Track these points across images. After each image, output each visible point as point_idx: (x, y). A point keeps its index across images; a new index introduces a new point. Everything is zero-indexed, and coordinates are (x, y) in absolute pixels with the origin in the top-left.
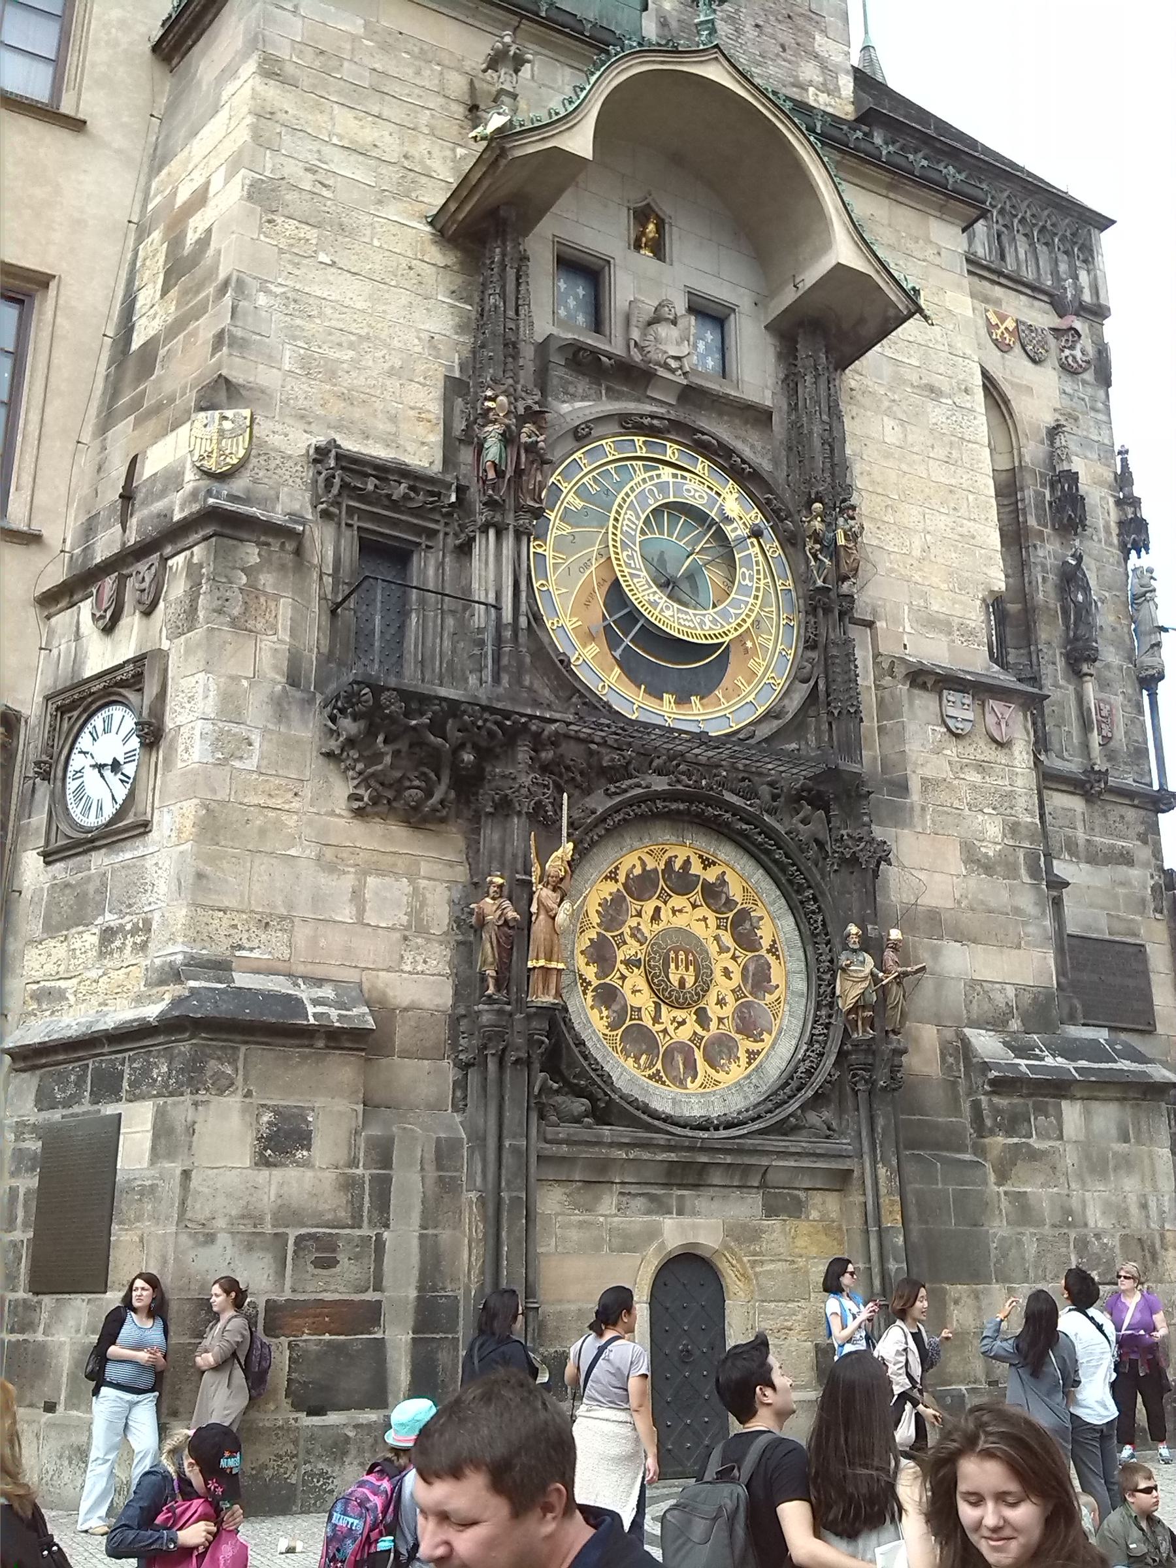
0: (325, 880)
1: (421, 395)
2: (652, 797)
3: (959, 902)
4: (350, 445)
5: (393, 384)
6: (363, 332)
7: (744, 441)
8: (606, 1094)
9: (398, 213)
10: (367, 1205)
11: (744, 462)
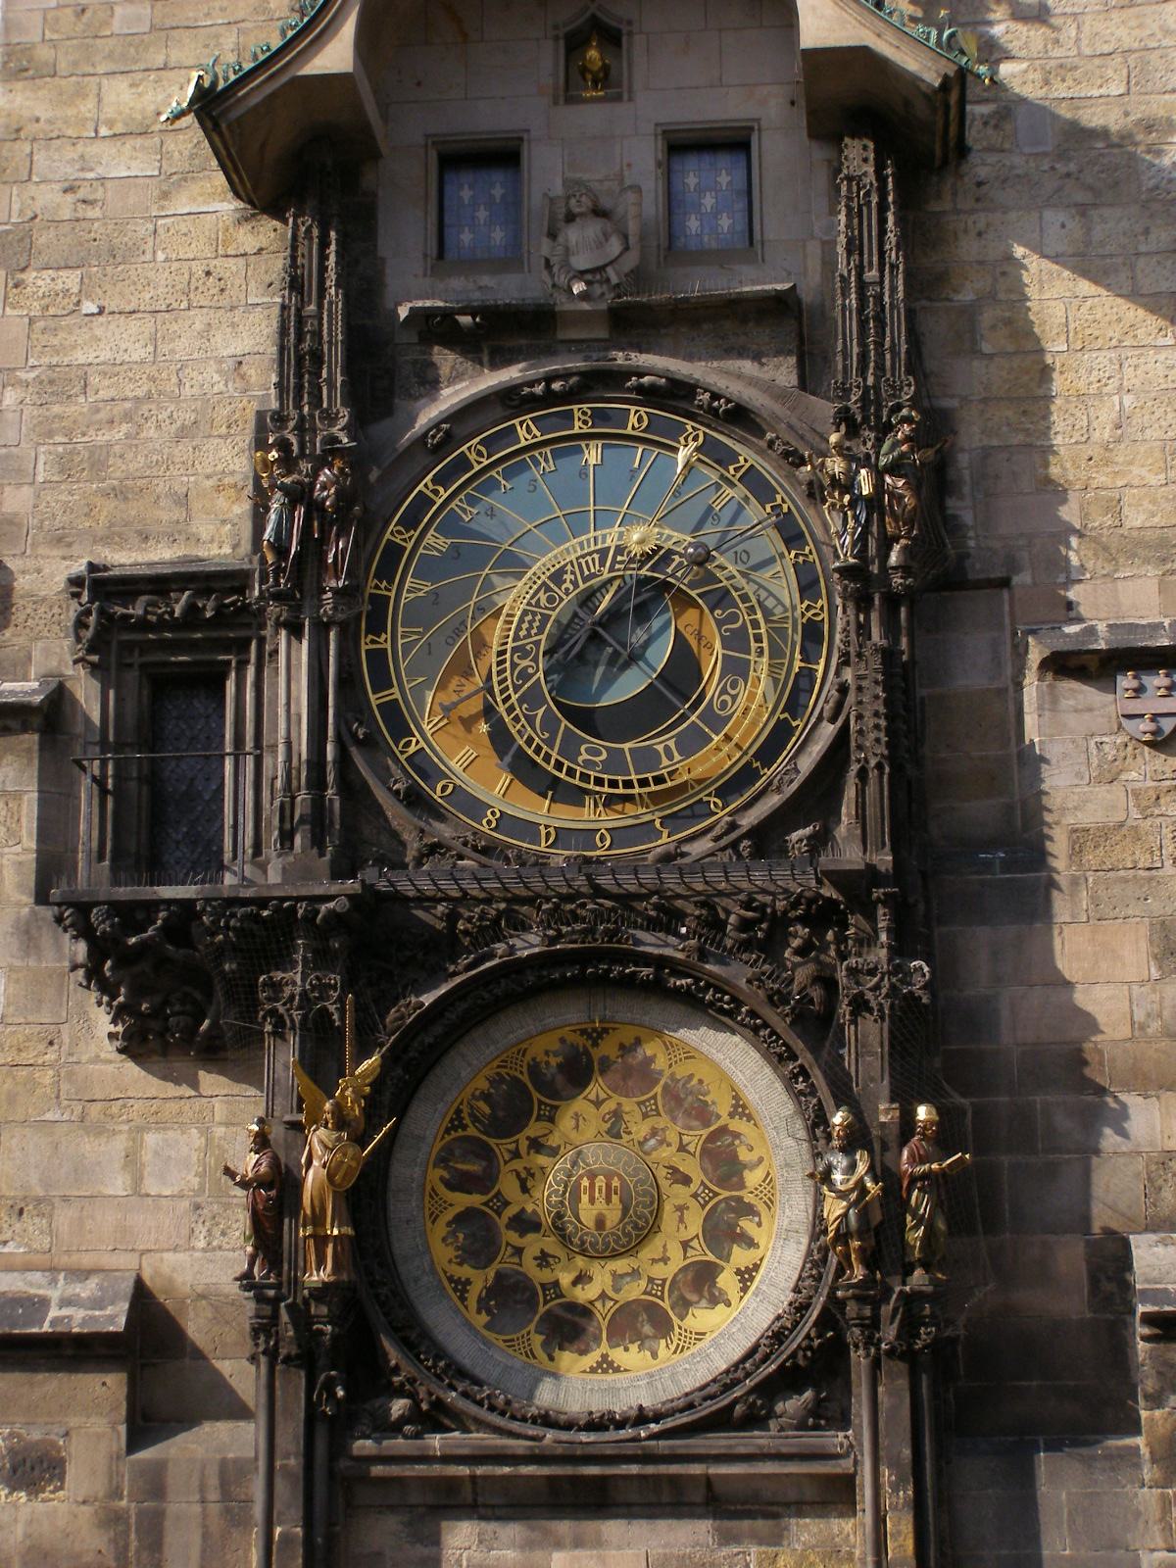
0: (89, 1147)
1: (224, 452)
2: (514, 968)
3: (1142, 1027)
4: (125, 559)
5: (183, 451)
6: (140, 393)
7: (741, 353)
8: (430, 1394)
9: (193, 200)
10: (134, 1544)
11: (715, 396)
